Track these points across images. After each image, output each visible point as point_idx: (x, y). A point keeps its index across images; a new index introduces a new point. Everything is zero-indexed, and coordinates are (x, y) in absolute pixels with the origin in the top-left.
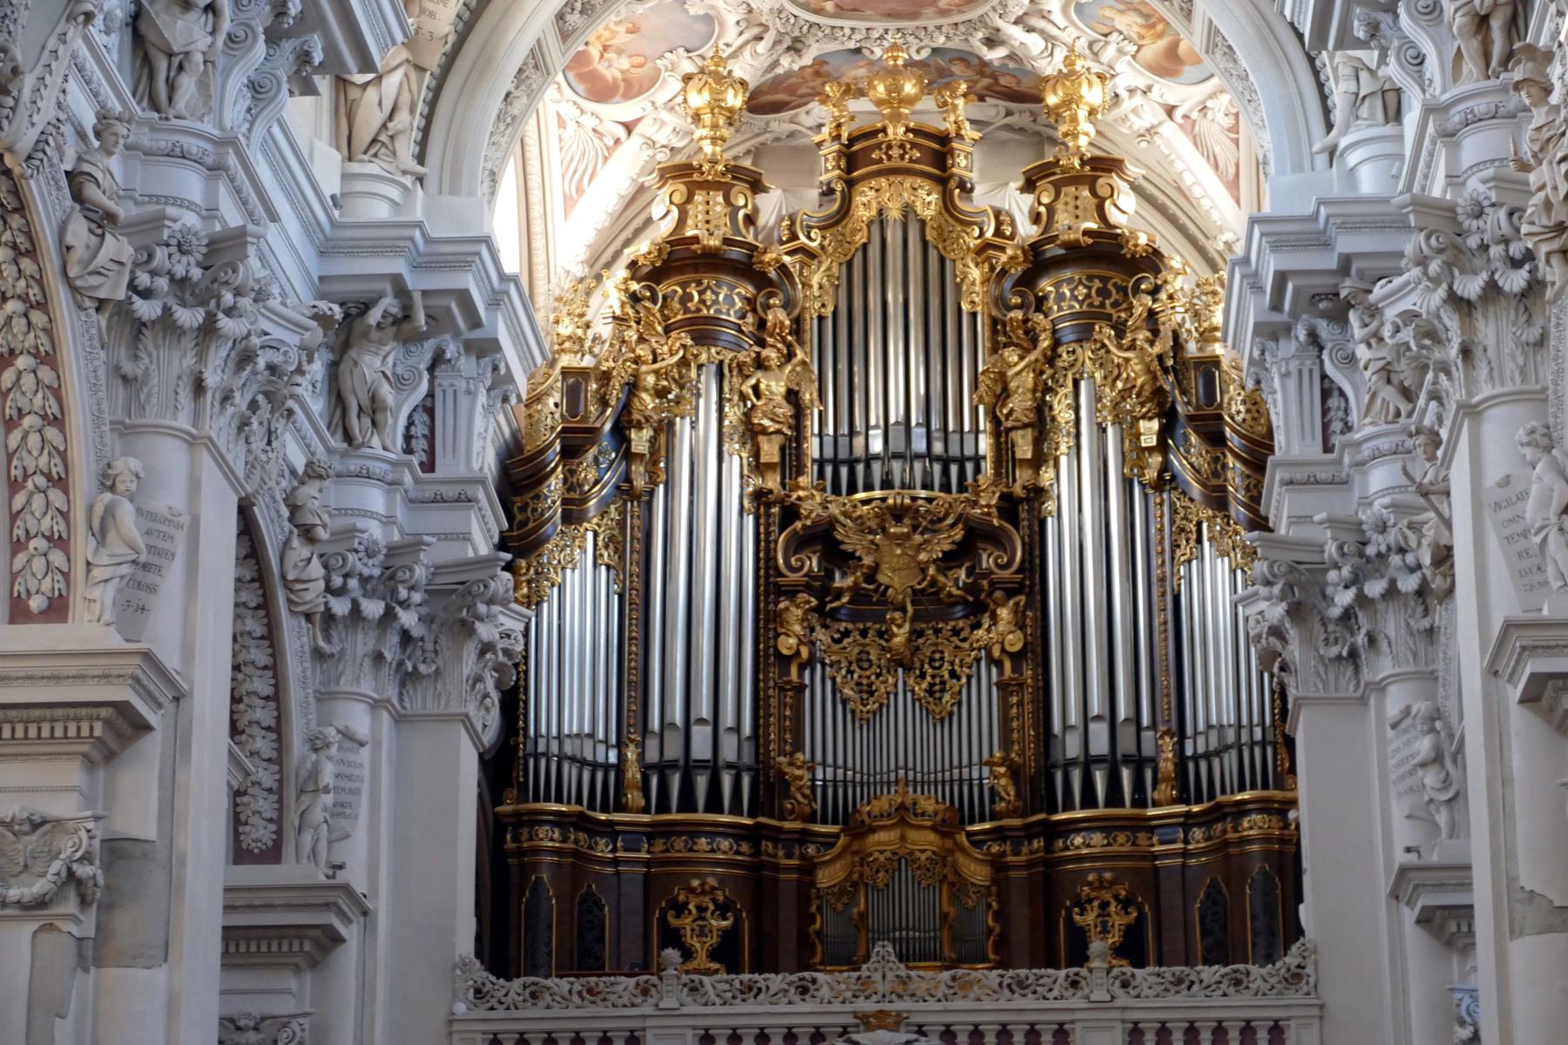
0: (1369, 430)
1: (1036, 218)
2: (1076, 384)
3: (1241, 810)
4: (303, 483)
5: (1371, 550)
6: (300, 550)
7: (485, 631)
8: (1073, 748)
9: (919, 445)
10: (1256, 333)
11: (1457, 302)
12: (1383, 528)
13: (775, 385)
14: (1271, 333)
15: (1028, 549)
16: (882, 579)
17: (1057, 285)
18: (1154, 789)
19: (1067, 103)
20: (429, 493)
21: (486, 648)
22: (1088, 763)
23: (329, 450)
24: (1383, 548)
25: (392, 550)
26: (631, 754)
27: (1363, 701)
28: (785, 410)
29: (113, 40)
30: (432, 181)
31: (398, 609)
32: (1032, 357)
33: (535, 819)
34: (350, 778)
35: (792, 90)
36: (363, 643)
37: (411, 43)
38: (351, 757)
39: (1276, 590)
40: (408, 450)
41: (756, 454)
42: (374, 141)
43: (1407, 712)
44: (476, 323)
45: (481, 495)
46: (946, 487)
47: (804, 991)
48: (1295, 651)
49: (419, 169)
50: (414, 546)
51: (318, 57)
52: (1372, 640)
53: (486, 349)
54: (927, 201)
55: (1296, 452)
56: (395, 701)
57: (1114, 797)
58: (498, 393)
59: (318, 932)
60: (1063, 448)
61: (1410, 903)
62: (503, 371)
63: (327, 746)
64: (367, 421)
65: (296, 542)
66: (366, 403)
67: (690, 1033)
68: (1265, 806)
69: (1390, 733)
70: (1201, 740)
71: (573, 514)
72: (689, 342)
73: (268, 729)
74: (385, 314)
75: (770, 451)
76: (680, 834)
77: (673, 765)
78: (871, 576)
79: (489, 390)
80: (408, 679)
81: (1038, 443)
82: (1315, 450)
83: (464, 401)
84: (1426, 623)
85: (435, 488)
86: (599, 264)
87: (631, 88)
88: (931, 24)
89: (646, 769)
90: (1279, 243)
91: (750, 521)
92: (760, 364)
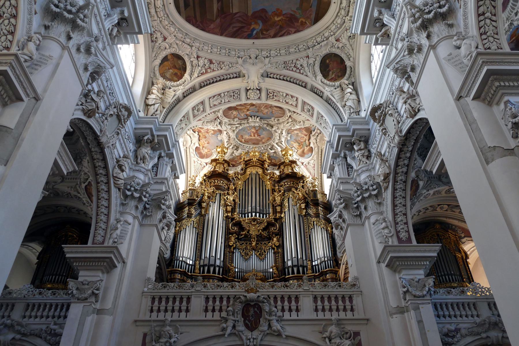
0: (360, 167)
1: (280, 172)
2: (288, 199)
3: (326, 273)
5: (364, 188)
6: (117, 170)
8: (290, 263)
9: (258, 210)
10: (332, 158)
12: (366, 184)
13: (232, 199)
14: (335, 157)
15: (280, 227)
16: (250, 233)
17: (284, 183)
18: (307, 271)
19: (286, 153)
22: (293, 266)
23: (132, 164)
24: (367, 187)
25: (143, 186)
26: (198, 262)
27: (363, 225)
28: (233, 202)
32: (280, 193)
33: (175, 272)
34: (125, 231)
35: (236, 162)
36: (133, 203)
37: (162, 100)
38: (126, 226)
39: (342, 201)
41: (227, 209)
43: (377, 220)
44: (169, 150)
46: (263, 217)
47: (232, 287)
48: (346, 215)
51: (126, 14)
52: (365, 208)
53: (170, 156)
54: (260, 171)
55: (342, 176)
57: (298, 272)
59: (107, 260)
60: (286, 210)
61: (384, 262)
63: (120, 221)
64: (142, 161)
66: (142, 158)
67: (203, 296)
68: (331, 272)
69: (372, 226)
70: (316, 262)
71: (190, 216)
73: (106, 215)
74: (148, 139)
76: (206, 278)
77: (206, 265)
78: (248, 232)
80: (145, 217)
81: (281, 209)
82: (347, 176)
83: (165, 166)
84: (379, 201)
87: (207, 156)
88: (261, 146)
89: (200, 266)
90: (339, 130)
91: (224, 222)
92: (228, 194)
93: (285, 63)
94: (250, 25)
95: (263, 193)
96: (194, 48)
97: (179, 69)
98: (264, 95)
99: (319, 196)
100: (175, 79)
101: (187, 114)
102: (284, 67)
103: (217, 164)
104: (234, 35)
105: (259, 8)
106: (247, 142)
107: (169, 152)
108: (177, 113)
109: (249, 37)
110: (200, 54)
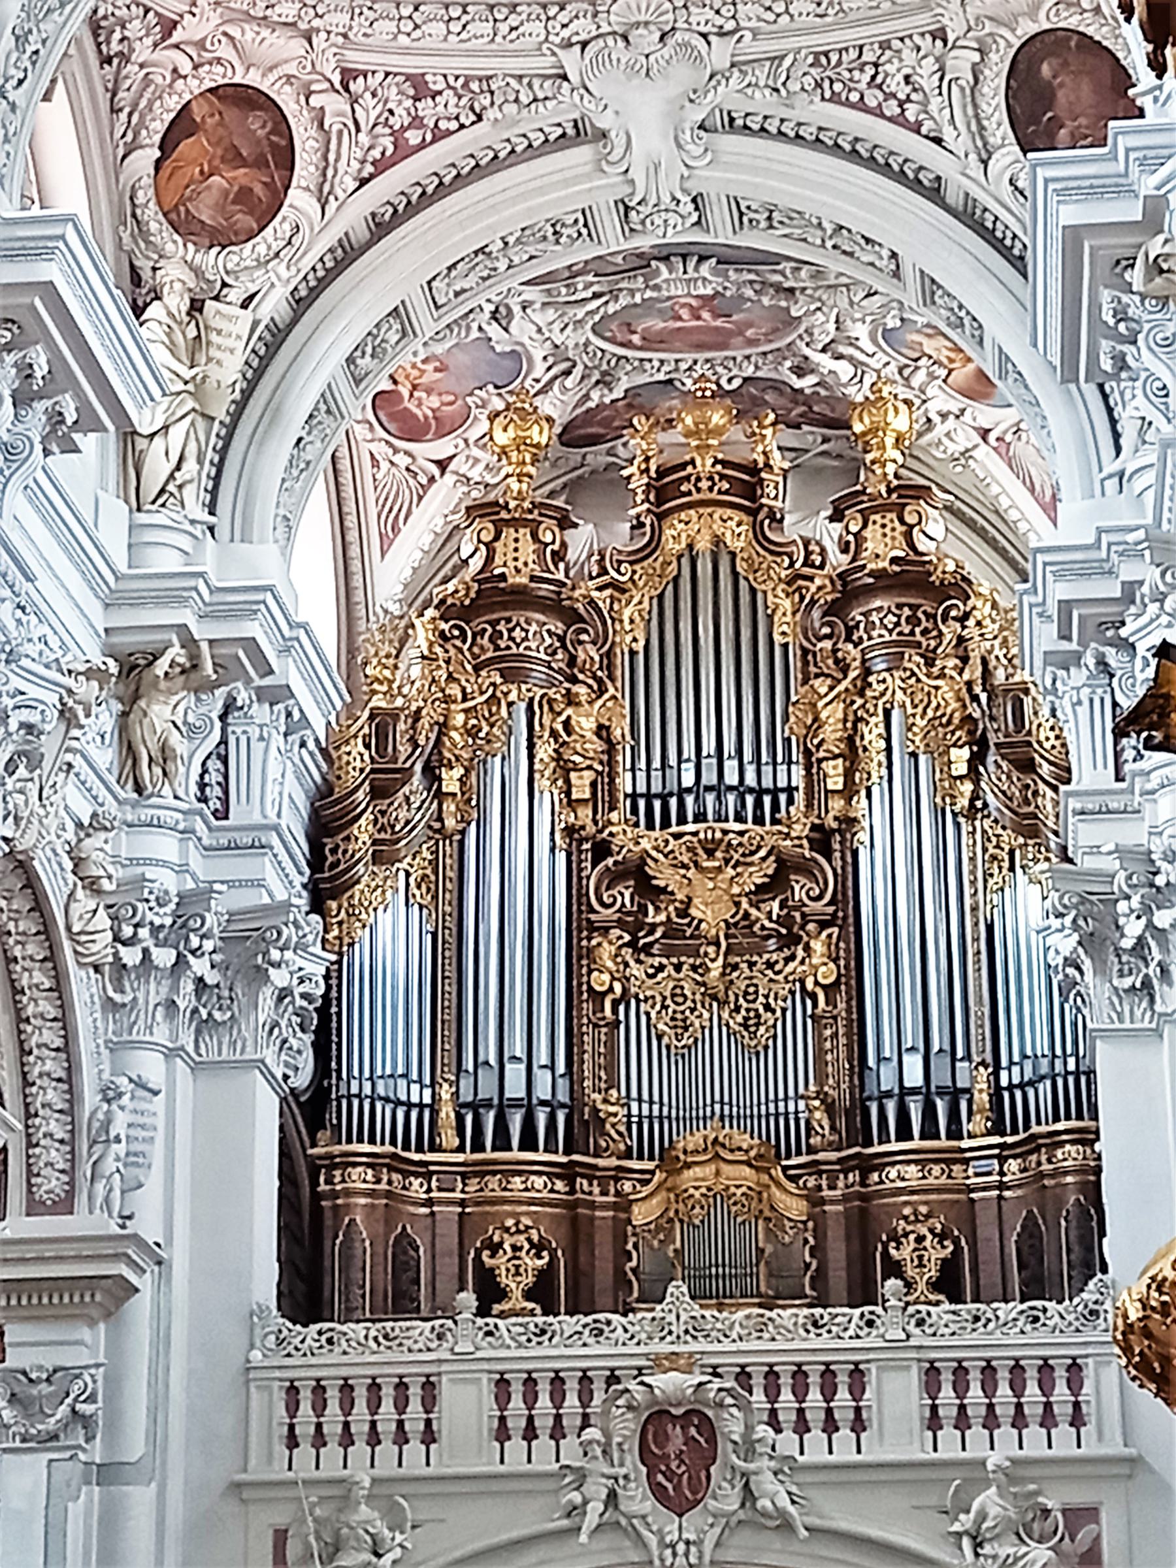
4: (88, 835)
7: (279, 978)
20: (224, 842)
21: (283, 994)
30: (223, 531)
31: (190, 957)
40: (203, 799)
42: (162, 491)
45: (275, 841)
49: (212, 519)
50: (204, 894)
56: (190, 1048)
58: (295, 738)
62: (296, 715)
65: (80, 894)
72: (499, 680)
79: (286, 735)
85: (230, 835)
93: (820, 57)
96: (319, 40)
102: (819, 85)
107: (268, 681)
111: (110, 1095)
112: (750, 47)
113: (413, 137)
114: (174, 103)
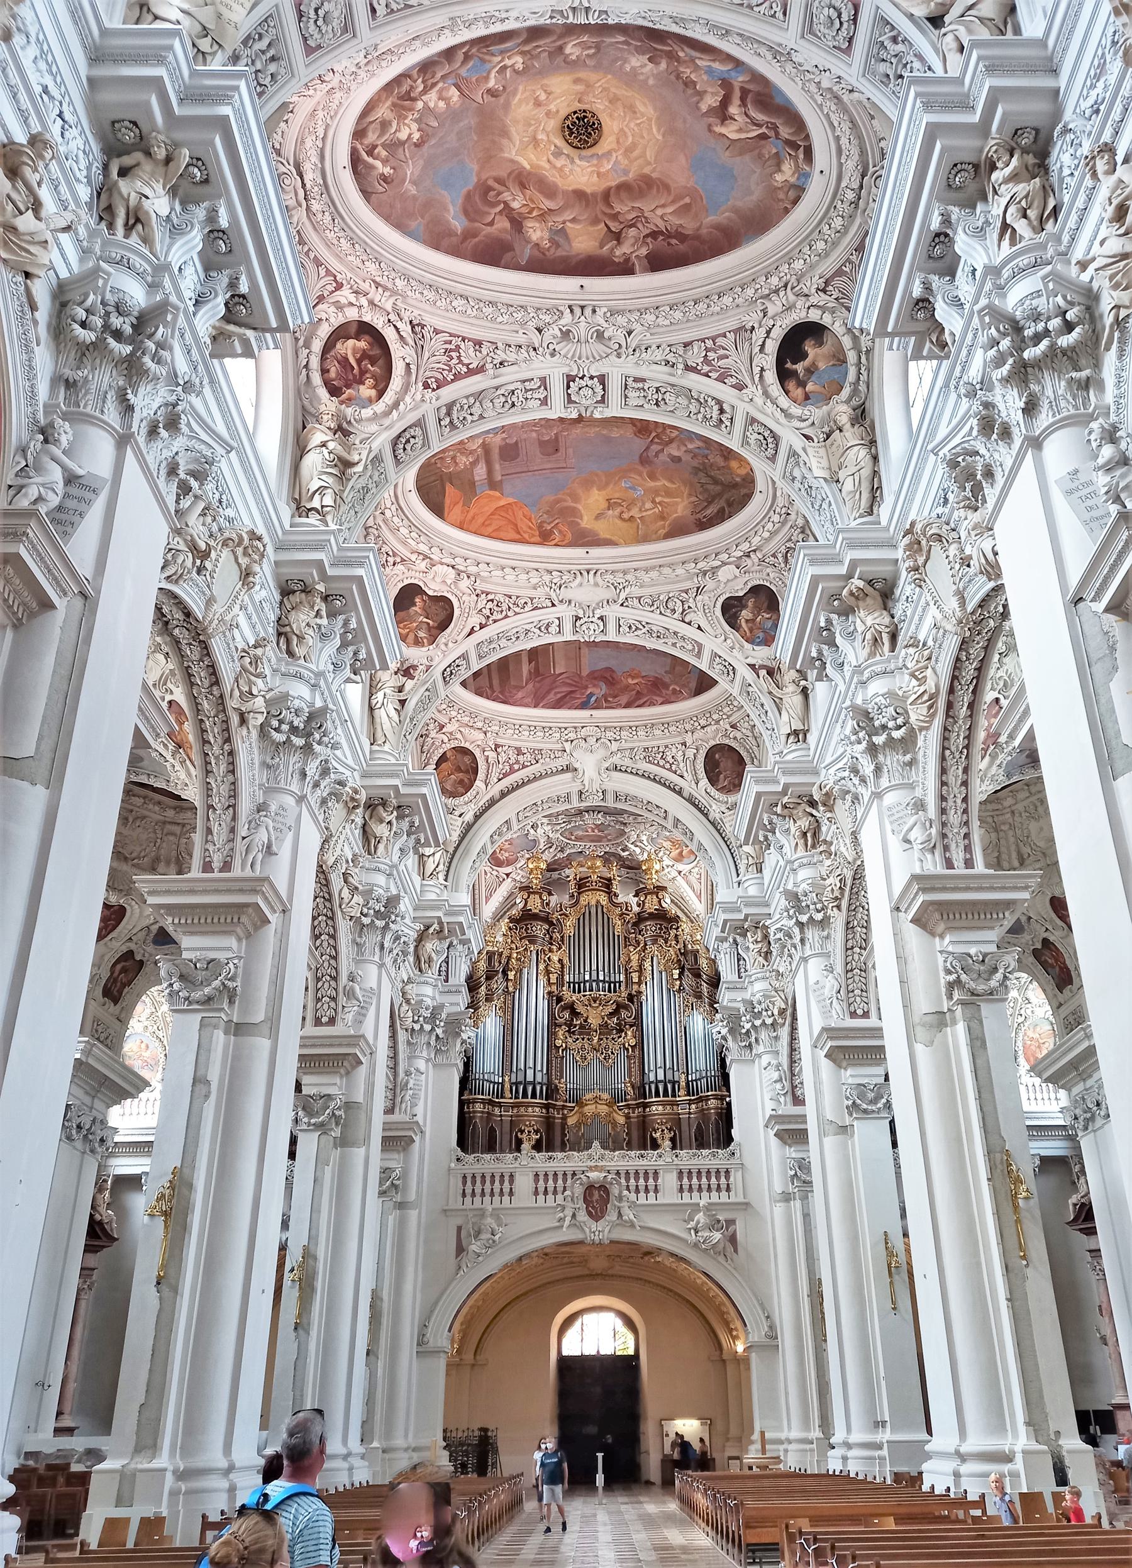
11: (800, 924)
13: (555, 958)
29: (357, 832)
53: (465, 942)
54: (603, 899)
71: (489, 999)
75: (553, 978)
86: (497, 917)
87: (509, 863)
92: (551, 950)
93: (646, 749)
94: (586, 687)
95: (610, 939)
97: (467, 772)
98: (610, 797)
99: (703, 963)
100: (461, 790)
101: (484, 848)
103: (529, 894)
104: (557, 705)
105: (602, 665)
106: (578, 839)
108: (467, 851)
109: (583, 706)
110: (500, 741)
111: (408, 1073)
112: (624, 745)
113: (516, 767)
114: (441, 751)
